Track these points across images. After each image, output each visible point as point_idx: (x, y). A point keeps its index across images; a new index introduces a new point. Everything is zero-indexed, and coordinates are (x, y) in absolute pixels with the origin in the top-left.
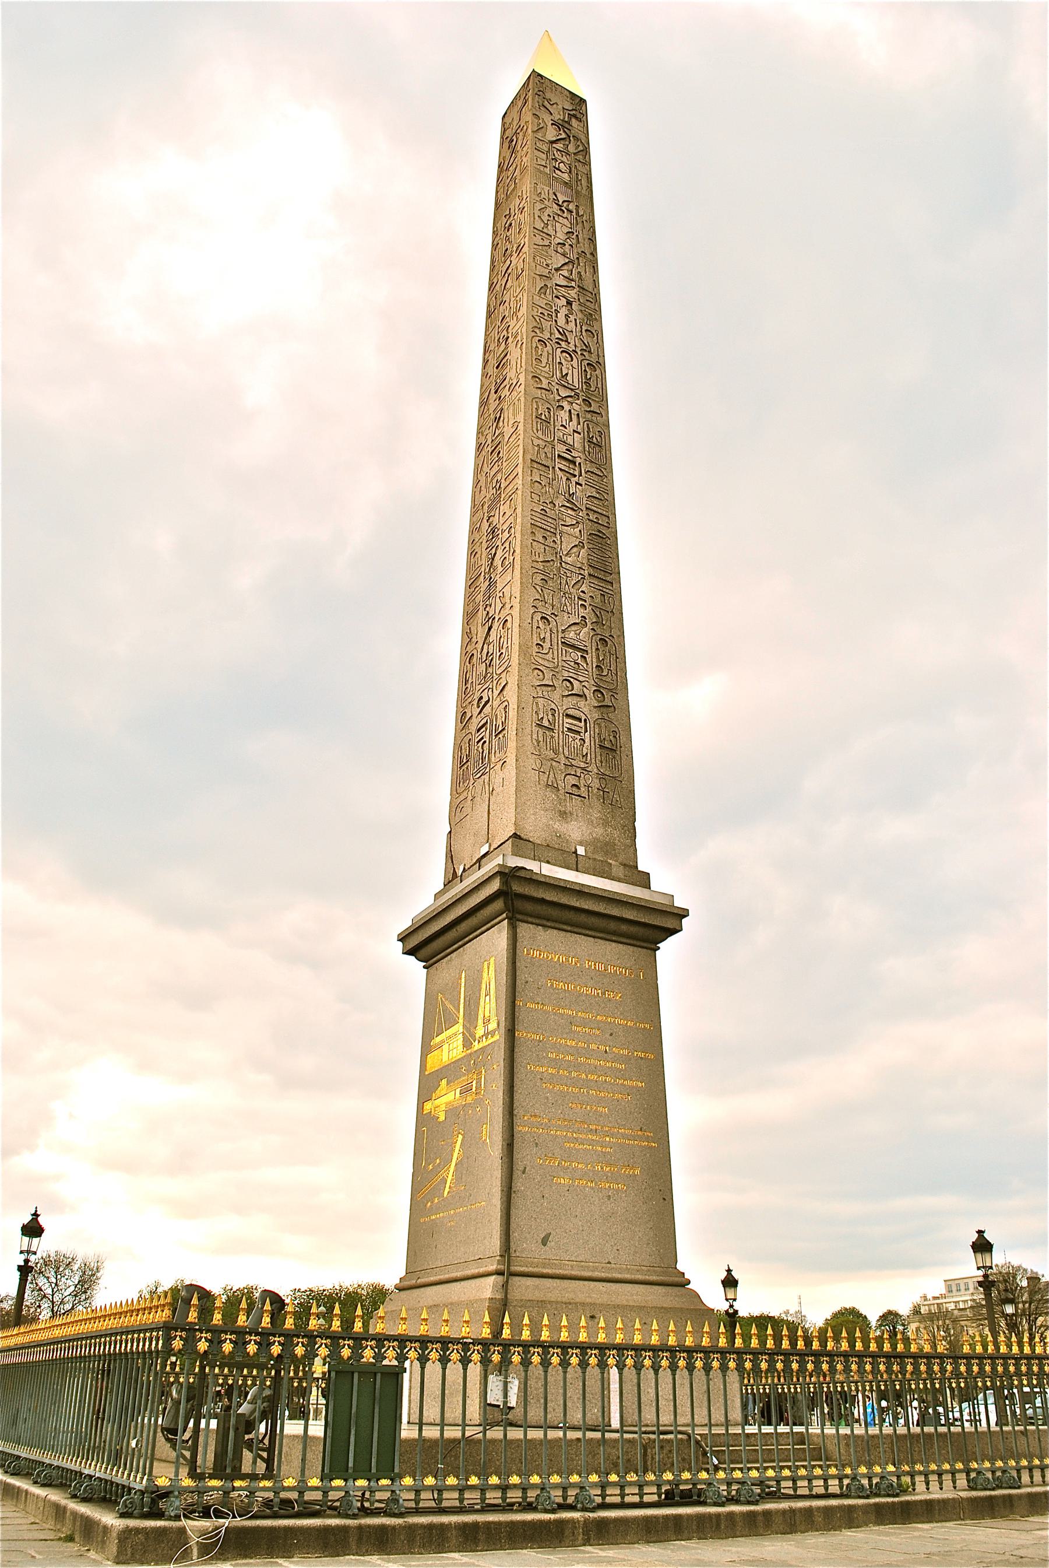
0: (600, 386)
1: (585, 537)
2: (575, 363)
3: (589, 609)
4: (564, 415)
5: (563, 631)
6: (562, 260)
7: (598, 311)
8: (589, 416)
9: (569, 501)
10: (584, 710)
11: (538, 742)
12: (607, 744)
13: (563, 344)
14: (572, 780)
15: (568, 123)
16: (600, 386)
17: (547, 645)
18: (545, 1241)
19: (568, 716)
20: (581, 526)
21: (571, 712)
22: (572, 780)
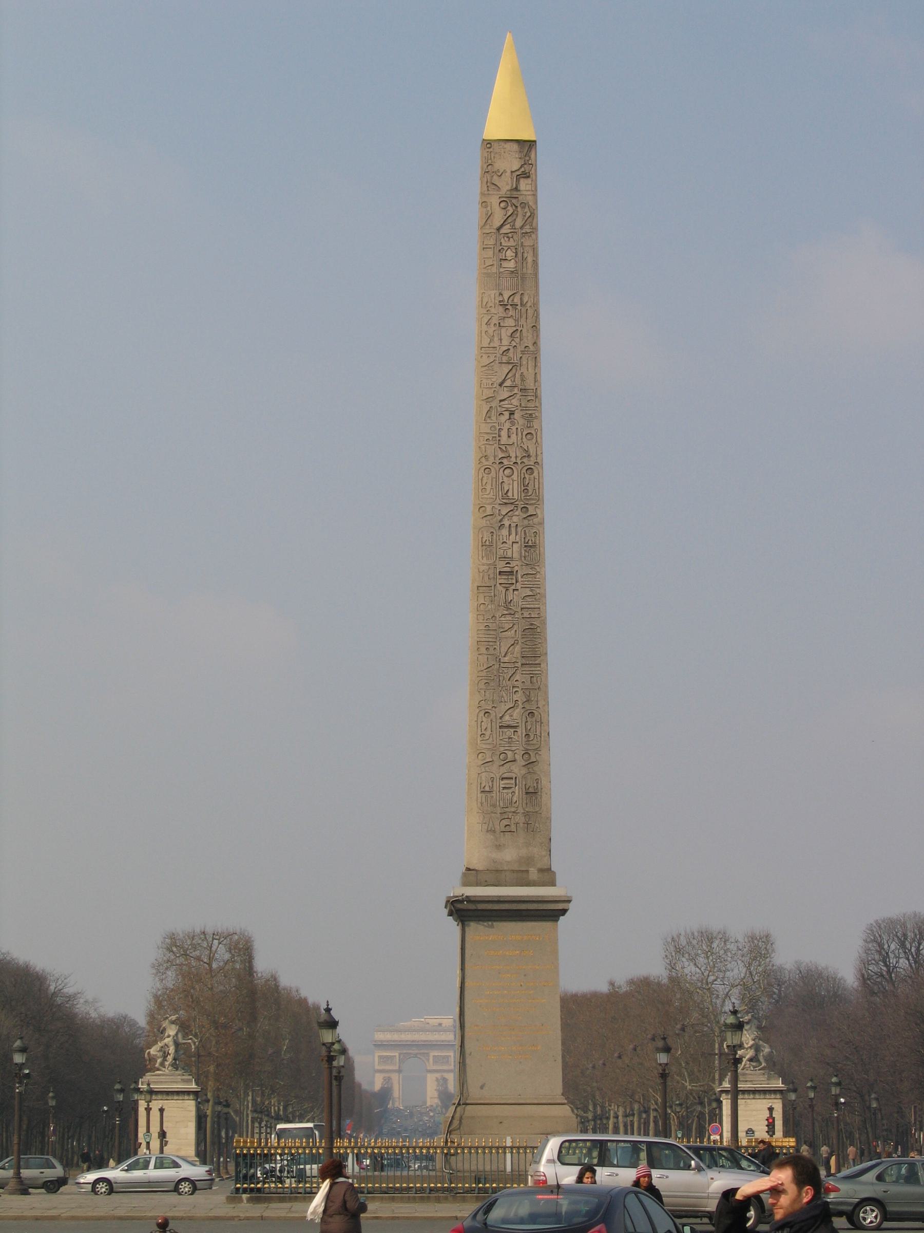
0: (537, 486)
1: (519, 633)
2: (515, 477)
3: (520, 692)
4: (505, 532)
5: (501, 718)
6: (505, 369)
7: (538, 408)
8: (526, 522)
9: (508, 609)
10: (516, 771)
11: (482, 804)
12: (531, 790)
13: (505, 462)
14: (505, 822)
15: (516, 189)
16: (537, 486)
17: (488, 733)
18: (482, 1087)
19: (503, 779)
20: (516, 627)
21: (505, 775)
22: (505, 822)
